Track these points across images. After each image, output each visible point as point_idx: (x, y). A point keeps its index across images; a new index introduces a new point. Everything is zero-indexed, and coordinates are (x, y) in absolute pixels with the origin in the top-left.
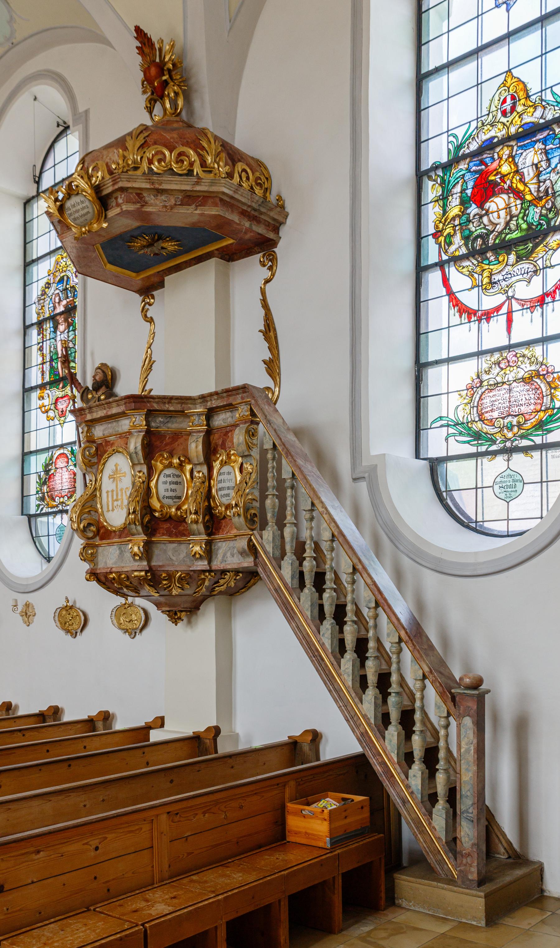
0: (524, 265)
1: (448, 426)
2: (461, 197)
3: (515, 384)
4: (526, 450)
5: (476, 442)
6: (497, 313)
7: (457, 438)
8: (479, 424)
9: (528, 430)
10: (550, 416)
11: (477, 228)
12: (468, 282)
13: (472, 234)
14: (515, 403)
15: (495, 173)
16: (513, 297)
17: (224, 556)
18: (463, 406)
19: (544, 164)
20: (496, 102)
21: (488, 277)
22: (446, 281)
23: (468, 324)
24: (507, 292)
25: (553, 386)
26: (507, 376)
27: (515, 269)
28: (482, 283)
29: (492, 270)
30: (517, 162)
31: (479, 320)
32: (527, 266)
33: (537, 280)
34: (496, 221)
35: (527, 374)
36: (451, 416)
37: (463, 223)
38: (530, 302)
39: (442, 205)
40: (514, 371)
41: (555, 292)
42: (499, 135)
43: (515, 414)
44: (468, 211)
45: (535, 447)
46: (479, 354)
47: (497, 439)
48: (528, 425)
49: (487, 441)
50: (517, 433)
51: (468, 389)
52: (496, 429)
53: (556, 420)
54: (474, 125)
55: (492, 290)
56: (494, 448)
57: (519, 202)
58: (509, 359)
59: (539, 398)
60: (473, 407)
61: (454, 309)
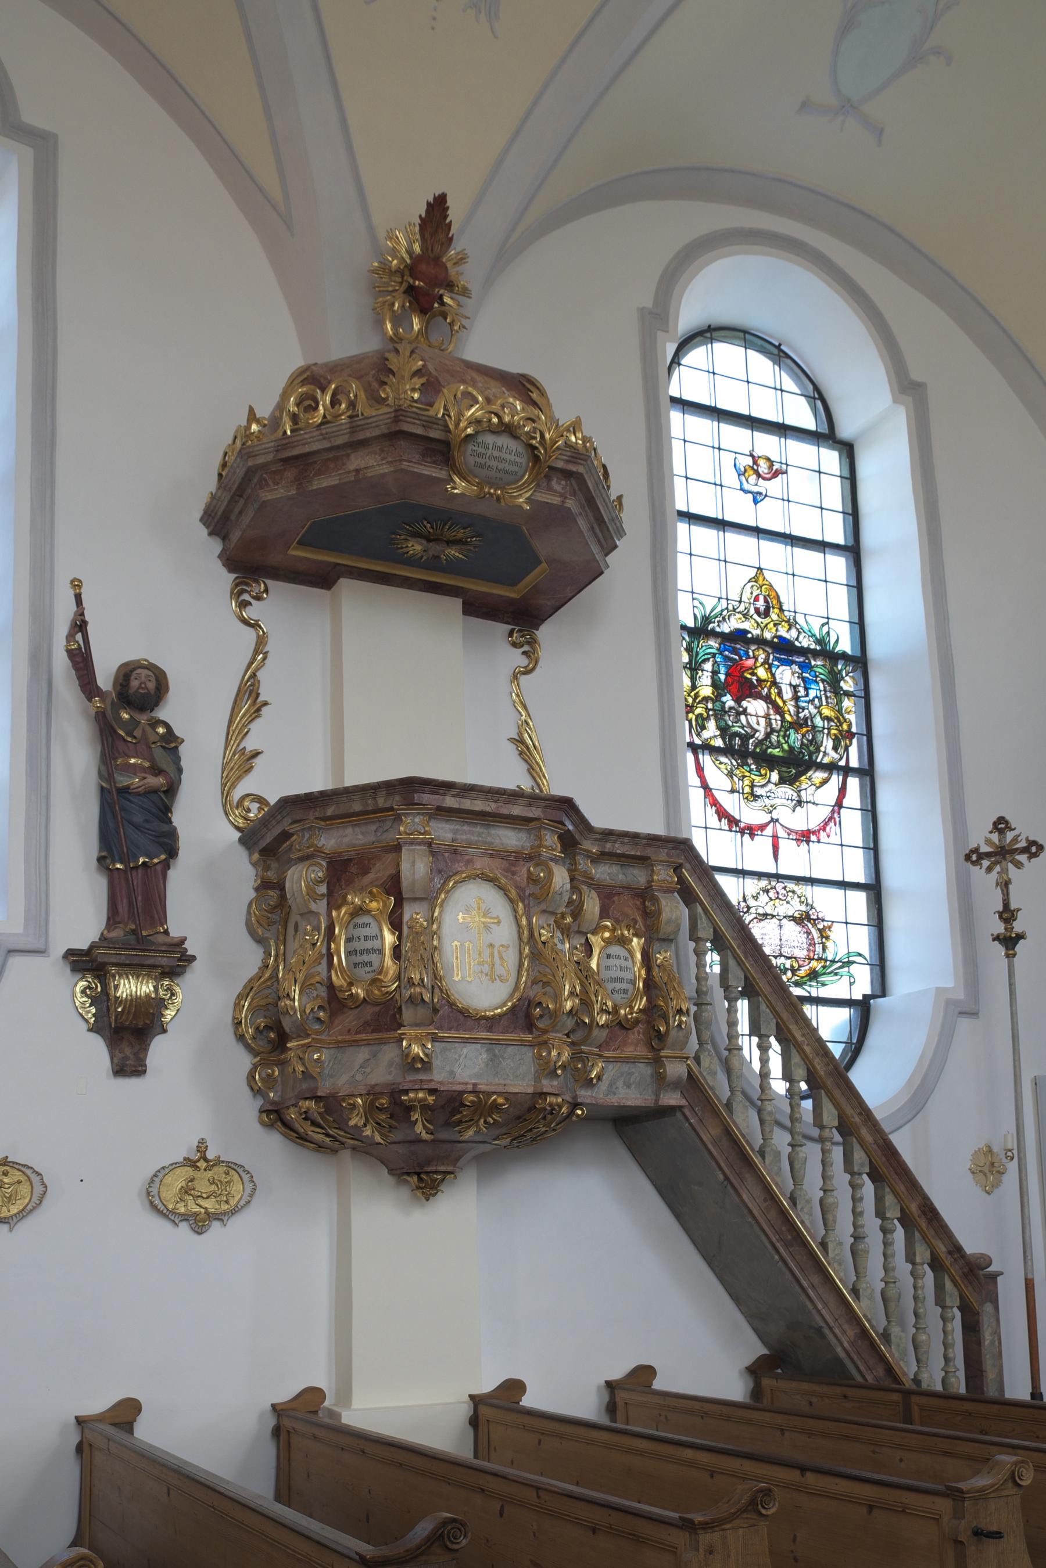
2: (712, 678)
9: (802, 977)
16: (777, 820)
17: (611, 1086)
20: (749, 595)
32: (792, 792)
34: (756, 726)
41: (819, 831)
44: (724, 699)
48: (802, 972)
53: (829, 973)
55: (753, 803)
57: (778, 717)
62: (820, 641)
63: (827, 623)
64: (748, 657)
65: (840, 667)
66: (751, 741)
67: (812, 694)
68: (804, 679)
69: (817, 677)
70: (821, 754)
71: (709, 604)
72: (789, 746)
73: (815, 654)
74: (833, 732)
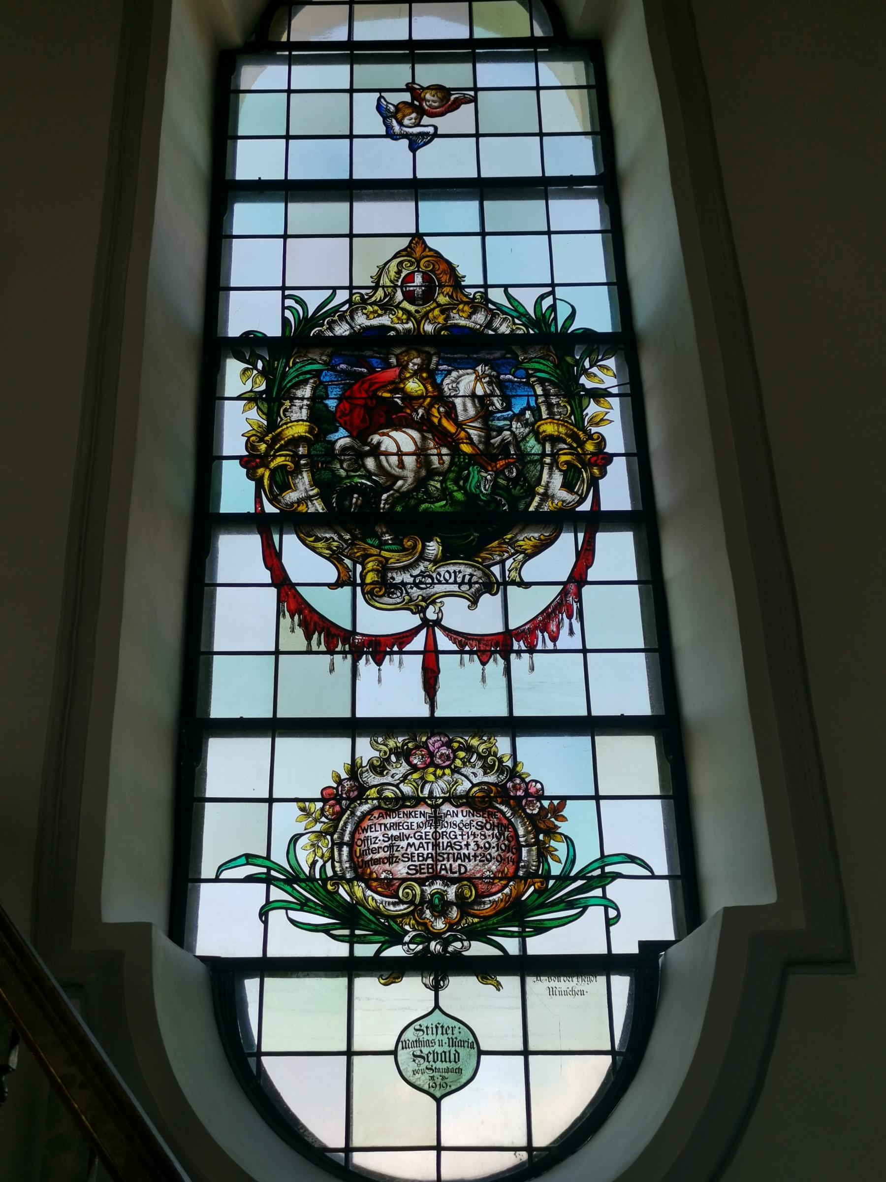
0: (462, 568)
1: (268, 880)
3: (446, 808)
5: (346, 932)
6: (400, 647)
8: (359, 889)
9: (486, 918)
11: (353, 474)
12: (330, 573)
16: (438, 623)
18: (312, 836)
19: (497, 403)
20: (392, 274)
21: (377, 570)
22: (272, 558)
23: (328, 657)
24: (423, 610)
26: (427, 788)
27: (442, 570)
29: (387, 559)
30: (439, 380)
32: (469, 571)
33: (490, 603)
34: (397, 471)
35: (475, 789)
36: (279, 856)
37: (318, 456)
38: (479, 641)
39: (265, 411)
40: (445, 778)
41: (532, 632)
42: (399, 327)
43: (450, 875)
44: (332, 437)
47: (407, 932)
48: (486, 907)
49: (376, 933)
50: (458, 923)
51: (324, 800)
52: (402, 907)
54: (342, 296)
55: (386, 599)
58: (431, 748)
59: (508, 849)
60: (340, 845)
61: (292, 617)
63: (552, 293)
64: (389, 366)
66: (384, 496)
67: (518, 405)
68: (501, 385)
69: (529, 376)
70: (537, 499)
71: (313, 300)
72: (466, 493)
73: (524, 342)
74: (563, 458)
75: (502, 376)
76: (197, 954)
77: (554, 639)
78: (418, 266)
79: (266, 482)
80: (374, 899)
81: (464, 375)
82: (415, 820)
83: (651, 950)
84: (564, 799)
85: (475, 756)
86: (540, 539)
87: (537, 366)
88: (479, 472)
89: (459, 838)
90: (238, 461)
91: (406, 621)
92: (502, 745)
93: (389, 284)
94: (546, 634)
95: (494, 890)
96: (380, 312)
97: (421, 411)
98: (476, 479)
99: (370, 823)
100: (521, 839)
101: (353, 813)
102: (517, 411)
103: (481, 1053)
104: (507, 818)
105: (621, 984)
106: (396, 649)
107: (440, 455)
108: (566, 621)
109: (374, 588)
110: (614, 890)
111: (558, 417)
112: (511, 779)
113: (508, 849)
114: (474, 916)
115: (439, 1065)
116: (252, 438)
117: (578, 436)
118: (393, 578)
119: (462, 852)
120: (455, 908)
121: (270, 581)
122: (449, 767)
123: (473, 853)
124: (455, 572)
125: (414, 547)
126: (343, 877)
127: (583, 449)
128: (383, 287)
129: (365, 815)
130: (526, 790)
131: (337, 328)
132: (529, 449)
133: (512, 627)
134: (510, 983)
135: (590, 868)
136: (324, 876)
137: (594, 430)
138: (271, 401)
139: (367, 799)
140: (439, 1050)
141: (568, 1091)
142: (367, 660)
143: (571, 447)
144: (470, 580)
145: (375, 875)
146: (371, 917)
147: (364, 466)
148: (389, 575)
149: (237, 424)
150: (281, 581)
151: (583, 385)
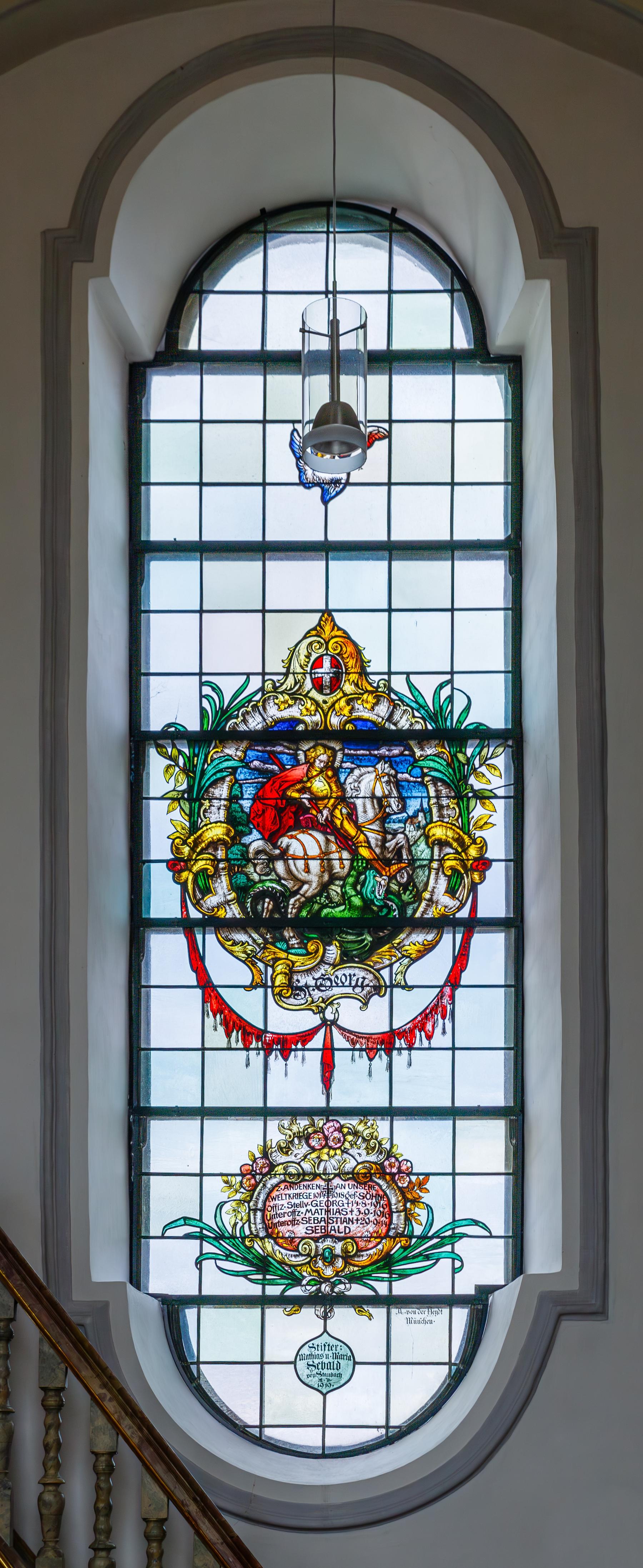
0: (357, 971)
1: (202, 1238)
2: (228, 809)
3: (337, 1181)
4: (358, 1302)
5: (260, 1277)
6: (304, 1044)
7: (221, 1264)
8: (269, 1245)
9: (363, 1267)
10: (405, 1248)
11: (264, 878)
12: (245, 976)
13: (252, 886)
14: (338, 1215)
15: (298, 786)
16: (334, 1022)
18: (234, 1204)
19: (394, 804)
20: (302, 658)
21: (285, 973)
22: (197, 960)
23: (244, 1053)
24: (322, 1011)
25: (409, 1196)
26: (322, 1164)
27: (339, 973)
28: (273, 982)
29: (293, 963)
30: (342, 780)
31: (268, 1050)
32: (362, 974)
33: (379, 1004)
34: (303, 876)
35: (360, 1166)
37: (234, 860)
38: (368, 1039)
39: (187, 812)
40: (337, 1157)
41: (412, 1031)
42: (307, 719)
43: (337, 1234)
44: (246, 840)
45: (376, 1300)
46: (265, 1113)
47: (304, 1277)
48: (364, 1259)
49: (282, 1277)
50: (343, 1270)
51: (243, 1175)
52: (301, 1258)
53: (414, 1257)
54: (256, 683)
55: (292, 1001)
56: (296, 1291)
57: (345, 855)
58: (326, 1133)
59: (383, 1214)
60: (255, 1210)
61: (215, 1017)
62: (434, 716)
63: (451, 681)
64: (297, 763)
65: (469, 751)
66: (292, 901)
67: (413, 806)
68: (398, 785)
69: (424, 775)
70: (423, 904)
71: (229, 686)
72: (363, 899)
73: (423, 737)
74: (448, 864)
75: (400, 776)
76: (150, 1292)
77: (429, 1037)
78: (327, 649)
79: (190, 886)
80: (281, 1253)
81: (365, 774)
82: (313, 1191)
83: (484, 1292)
84: (428, 1175)
85: (360, 1139)
86: (423, 944)
87: (432, 764)
88: (375, 876)
89: (346, 1206)
90: (165, 864)
91: (308, 1020)
92: (382, 1127)
93: (299, 670)
94: (423, 1033)
95: (370, 1246)
96: (290, 702)
97: (325, 812)
98: (371, 884)
99: (278, 1193)
100: (393, 1207)
101: (264, 1185)
102: (411, 813)
103: (355, 1363)
104: (383, 1191)
105: (461, 1315)
106: (299, 1046)
107: (341, 859)
108: (440, 1021)
109: (281, 991)
110: (461, 1247)
111: (446, 820)
112: (387, 1159)
113: (383, 1214)
114: (354, 1265)
115: (325, 1371)
116: (177, 841)
117: (463, 840)
118: (298, 981)
119: (347, 1217)
120: (340, 1260)
121: (195, 984)
122: (340, 1148)
123: (355, 1218)
124: (350, 975)
125: (317, 951)
126: (257, 1236)
127: (466, 854)
128: (294, 673)
129: (274, 1187)
130: (399, 1168)
131: (250, 720)
132: (419, 853)
133: (395, 1027)
134: (379, 1313)
135: (443, 1230)
136: (243, 1235)
137: (478, 834)
138: (193, 798)
139: (275, 1175)
140: (326, 1361)
141: (415, 1390)
142: (276, 1056)
143: (457, 852)
144: (362, 983)
145: (281, 1235)
146: (278, 1266)
147: (274, 870)
148: (295, 977)
149: (163, 824)
150: (205, 983)
151: (472, 786)
